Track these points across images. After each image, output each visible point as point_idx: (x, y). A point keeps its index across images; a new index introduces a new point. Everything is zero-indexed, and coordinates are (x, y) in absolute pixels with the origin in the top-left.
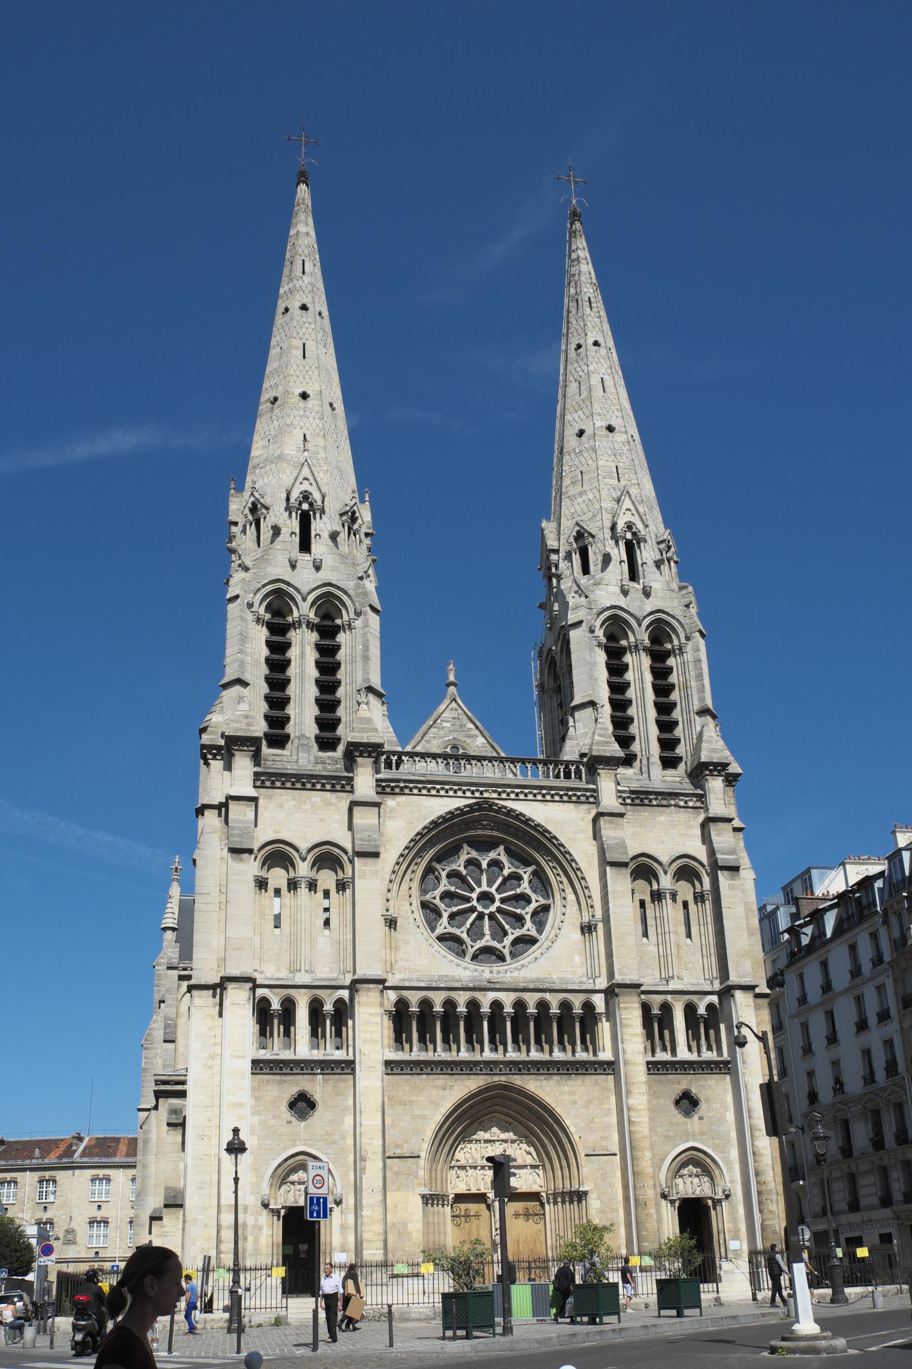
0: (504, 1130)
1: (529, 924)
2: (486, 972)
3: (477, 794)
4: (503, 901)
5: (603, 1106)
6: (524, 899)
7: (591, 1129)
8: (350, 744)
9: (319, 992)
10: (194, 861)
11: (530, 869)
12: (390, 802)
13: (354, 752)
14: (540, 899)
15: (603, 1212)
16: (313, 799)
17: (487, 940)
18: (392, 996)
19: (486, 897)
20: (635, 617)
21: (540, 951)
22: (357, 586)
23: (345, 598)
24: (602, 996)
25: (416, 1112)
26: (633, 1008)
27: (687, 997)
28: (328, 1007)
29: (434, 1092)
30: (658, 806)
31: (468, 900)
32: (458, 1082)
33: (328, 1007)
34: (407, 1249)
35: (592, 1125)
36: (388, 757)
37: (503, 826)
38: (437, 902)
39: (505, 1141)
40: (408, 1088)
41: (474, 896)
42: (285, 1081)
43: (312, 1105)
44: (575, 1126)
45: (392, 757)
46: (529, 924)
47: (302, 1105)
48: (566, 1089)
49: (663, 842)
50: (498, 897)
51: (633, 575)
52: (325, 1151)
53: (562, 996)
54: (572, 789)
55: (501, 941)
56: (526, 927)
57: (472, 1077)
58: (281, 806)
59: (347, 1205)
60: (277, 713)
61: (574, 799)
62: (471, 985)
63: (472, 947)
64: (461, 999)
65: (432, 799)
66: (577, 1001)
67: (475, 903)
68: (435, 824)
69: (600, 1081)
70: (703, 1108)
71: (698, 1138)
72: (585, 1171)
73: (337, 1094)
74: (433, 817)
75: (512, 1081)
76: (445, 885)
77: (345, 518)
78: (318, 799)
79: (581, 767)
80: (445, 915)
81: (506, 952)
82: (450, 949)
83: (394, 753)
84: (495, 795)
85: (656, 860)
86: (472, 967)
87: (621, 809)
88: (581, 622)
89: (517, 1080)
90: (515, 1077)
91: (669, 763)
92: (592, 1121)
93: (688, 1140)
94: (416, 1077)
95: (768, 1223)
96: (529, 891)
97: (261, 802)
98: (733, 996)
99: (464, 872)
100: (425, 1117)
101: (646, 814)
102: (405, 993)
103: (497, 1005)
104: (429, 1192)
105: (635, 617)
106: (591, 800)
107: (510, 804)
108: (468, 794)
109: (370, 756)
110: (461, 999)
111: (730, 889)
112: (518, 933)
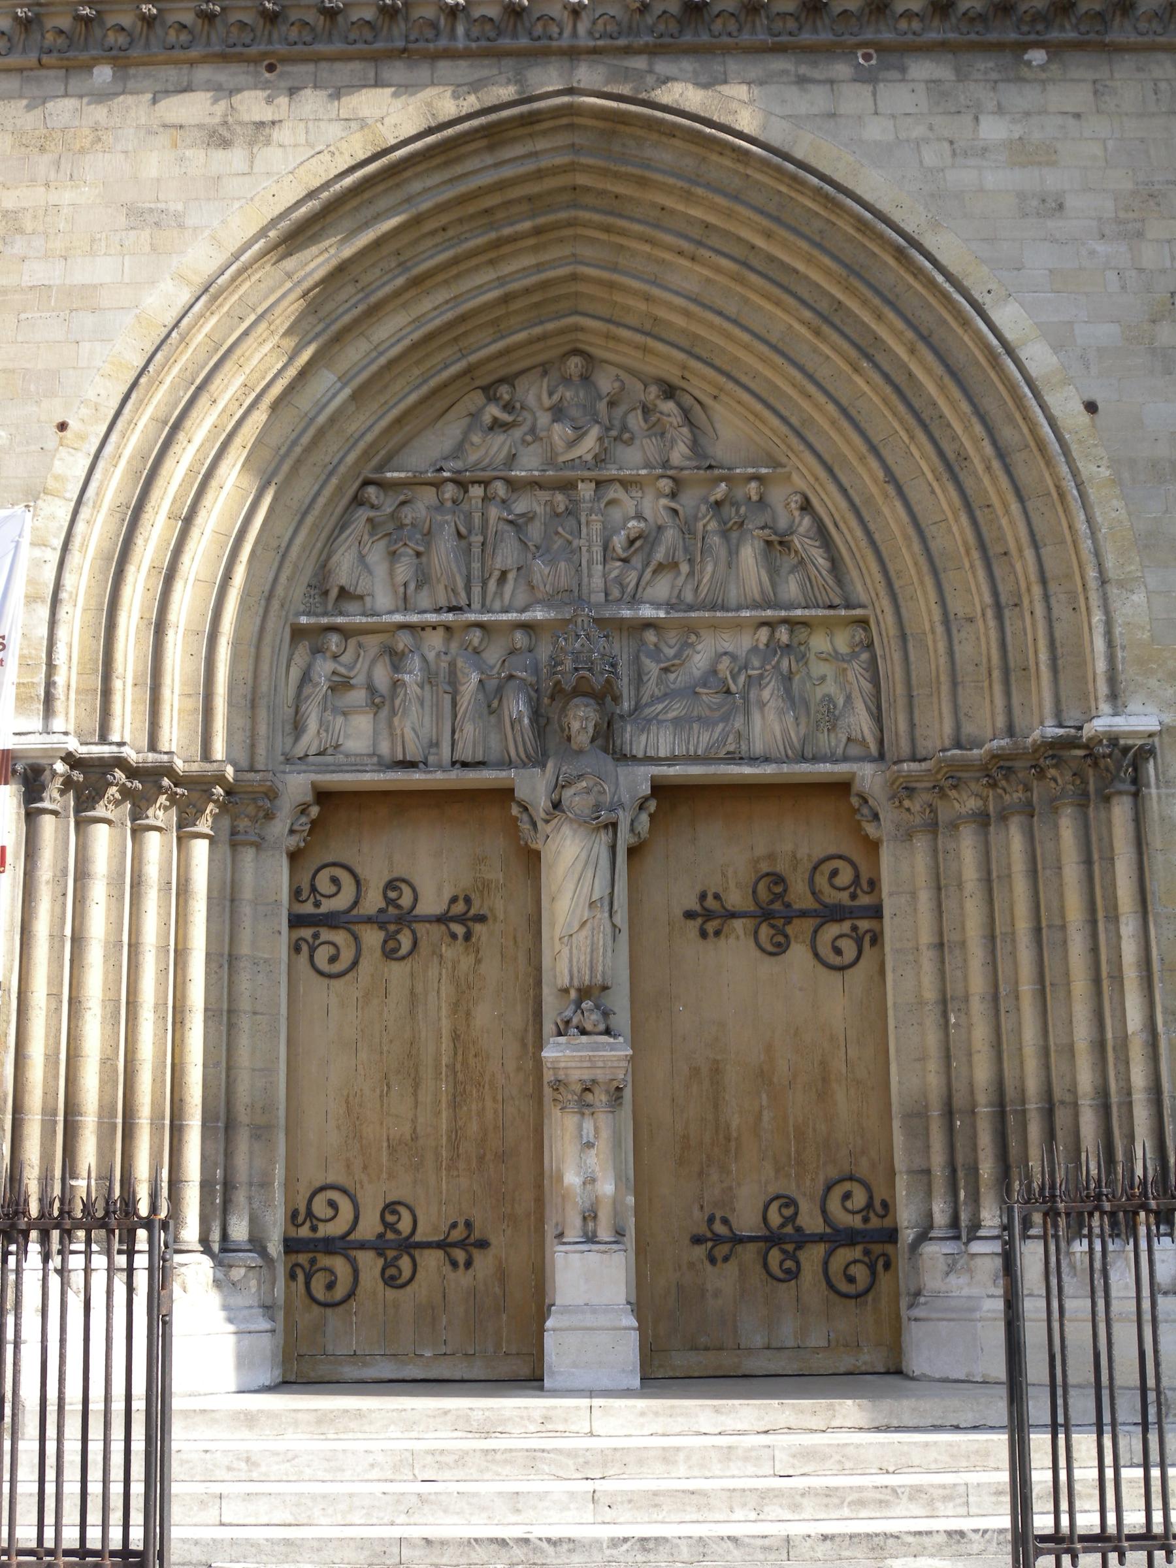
29: (155, 162)
48: (993, 130)
100: (82, 299)
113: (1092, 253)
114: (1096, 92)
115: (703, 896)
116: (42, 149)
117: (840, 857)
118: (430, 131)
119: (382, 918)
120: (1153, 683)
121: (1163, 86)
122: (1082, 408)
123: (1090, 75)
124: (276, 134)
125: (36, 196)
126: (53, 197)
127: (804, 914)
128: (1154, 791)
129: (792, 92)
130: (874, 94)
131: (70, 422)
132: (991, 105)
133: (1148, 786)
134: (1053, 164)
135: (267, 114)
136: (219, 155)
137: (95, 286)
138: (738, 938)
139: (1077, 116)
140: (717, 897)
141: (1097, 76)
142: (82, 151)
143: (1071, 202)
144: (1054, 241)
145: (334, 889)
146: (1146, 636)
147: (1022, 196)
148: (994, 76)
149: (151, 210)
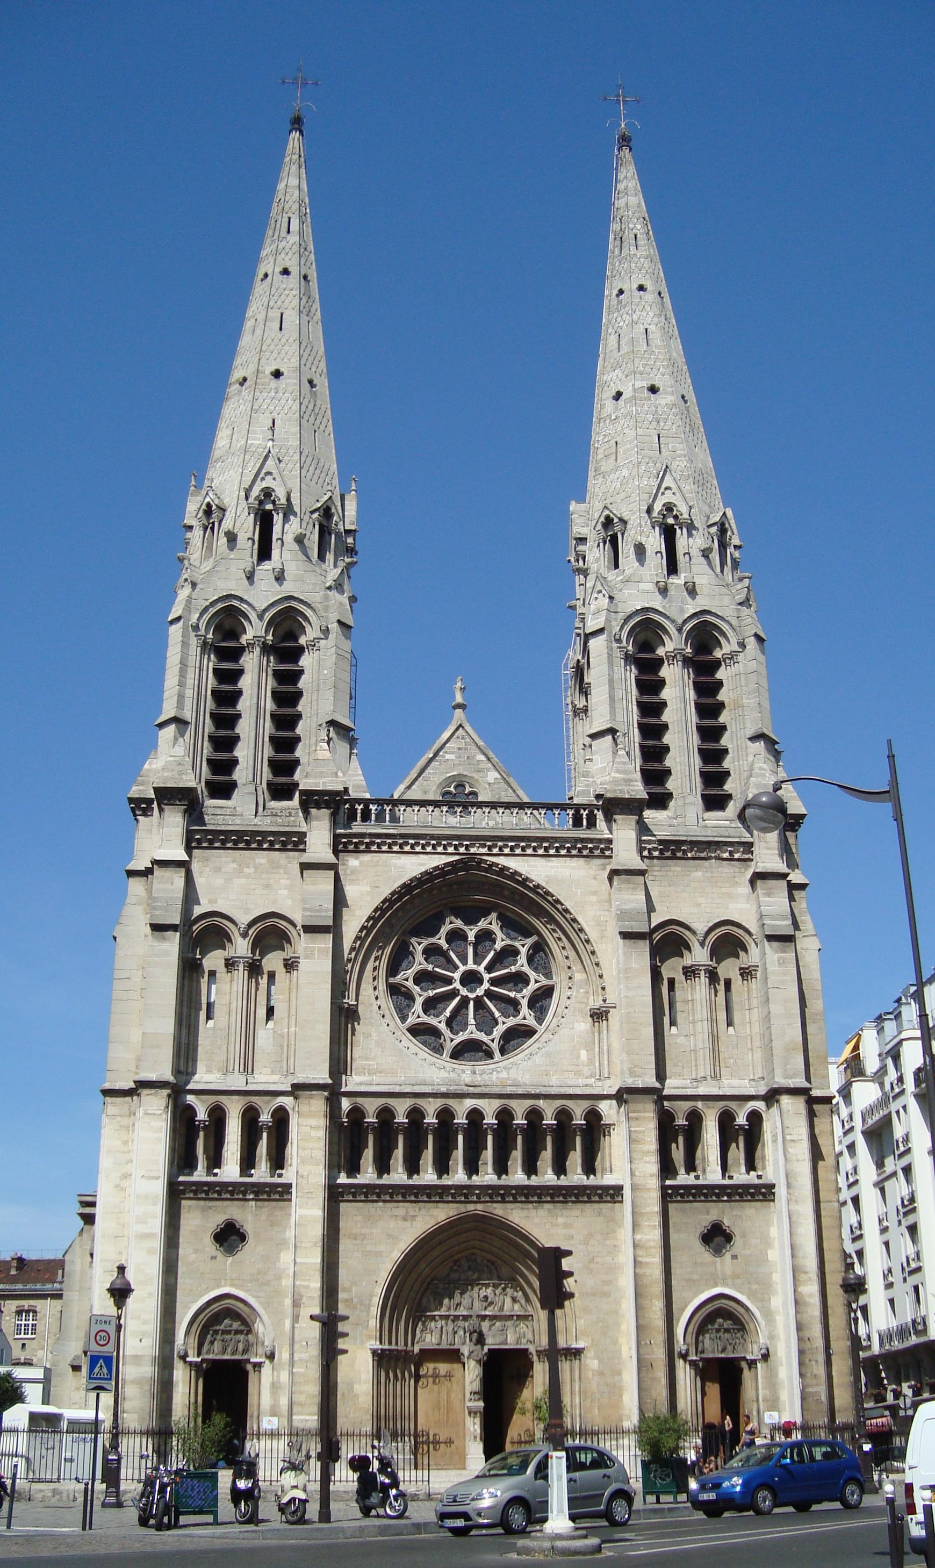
1: (525, 1010)
2: (466, 1074)
3: (462, 850)
4: (493, 982)
5: (608, 1242)
6: (520, 979)
7: (591, 1271)
8: (303, 793)
9: (254, 1099)
10: (115, 938)
11: (530, 941)
12: (352, 862)
13: (311, 800)
14: (542, 978)
15: (601, 1374)
16: (257, 861)
17: (472, 1032)
18: (346, 1104)
19: (471, 979)
20: (673, 621)
21: (536, 1045)
22: (326, 598)
23: (309, 613)
24: (614, 1102)
25: (369, 1248)
26: (645, 1118)
27: (722, 1104)
28: (265, 1118)
29: (392, 1224)
30: (693, 858)
31: (449, 981)
32: (423, 1212)
33: (265, 1118)
34: (352, 1415)
35: (592, 1266)
36: (352, 806)
37: (496, 889)
38: (410, 984)
40: (359, 1218)
41: (457, 976)
42: (210, 1208)
43: (243, 1238)
45: (357, 806)
46: (525, 1010)
47: (229, 1237)
48: (560, 1220)
49: (699, 905)
50: (487, 977)
51: (672, 569)
52: (256, 1294)
53: (559, 1103)
54: (582, 840)
55: (489, 1033)
56: (521, 1016)
57: (440, 1205)
58: (218, 869)
59: (280, 1359)
60: (224, 756)
61: (585, 852)
62: (444, 1089)
63: (452, 1040)
64: (431, 1108)
65: (403, 856)
66: (578, 1111)
67: (457, 985)
68: (407, 888)
69: (604, 1211)
70: (738, 1241)
71: (730, 1281)
73: (272, 1224)
74: (405, 879)
75: (491, 1210)
76: (420, 963)
77: (316, 515)
78: (263, 861)
79: (596, 811)
80: (419, 1001)
81: (495, 1046)
82: (424, 1043)
83: (359, 801)
84: (485, 850)
85: (688, 928)
86: (451, 1064)
87: (641, 865)
88: (601, 631)
89: (498, 1210)
90: (495, 1205)
91: (715, 801)
92: (591, 1261)
93: (716, 1285)
94: (370, 1204)
95: (810, 1390)
96: (526, 969)
97: (195, 867)
98: (778, 1101)
99: (445, 946)
100: (379, 1254)
101: (678, 869)
102: (360, 1100)
103: (475, 1116)
104: (380, 1347)
105: (673, 621)
106: (607, 853)
107: (502, 861)
108: (451, 850)
109: (327, 808)
110: (431, 1108)
111: (779, 964)
112: (511, 1022)
129: (520, 1211)
136: (405, 1223)
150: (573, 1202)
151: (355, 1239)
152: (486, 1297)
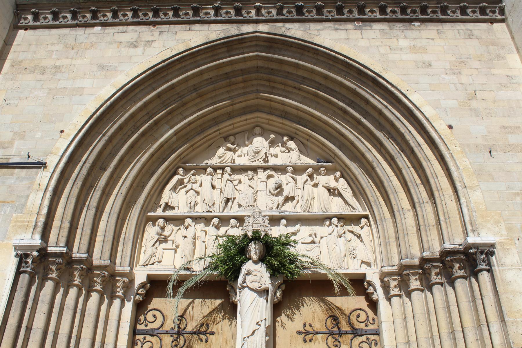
0: (278, 137)
5: (494, 71)
7: (476, 112)
29: (111, 52)
35: (474, 104)
39: (281, 169)
44: (436, 105)
48: (403, 43)
57: (197, 27)
72: (475, 197)
90: (288, 25)
100: (79, 91)
113: (444, 79)
114: (438, 33)
115: (305, 325)
116: (73, 48)
117: (360, 309)
118: (207, 43)
119: (172, 332)
120: (489, 225)
121: (461, 31)
122: (447, 127)
123: (436, 28)
124: (153, 44)
125: (67, 62)
126: (74, 62)
127: (346, 333)
128: (496, 268)
129: (334, 32)
130: (362, 33)
131: (65, 130)
132: (403, 36)
133: (494, 266)
134: (426, 53)
135: (151, 39)
137: (83, 88)
138: (319, 342)
139: (433, 39)
140: (310, 325)
141: (438, 29)
142: (86, 49)
143: (433, 64)
144: (429, 75)
145: (154, 319)
146: (484, 207)
147: (416, 62)
148: (402, 28)
149: (107, 66)
150: (422, 21)
151: (43, 73)
152: (279, 188)
